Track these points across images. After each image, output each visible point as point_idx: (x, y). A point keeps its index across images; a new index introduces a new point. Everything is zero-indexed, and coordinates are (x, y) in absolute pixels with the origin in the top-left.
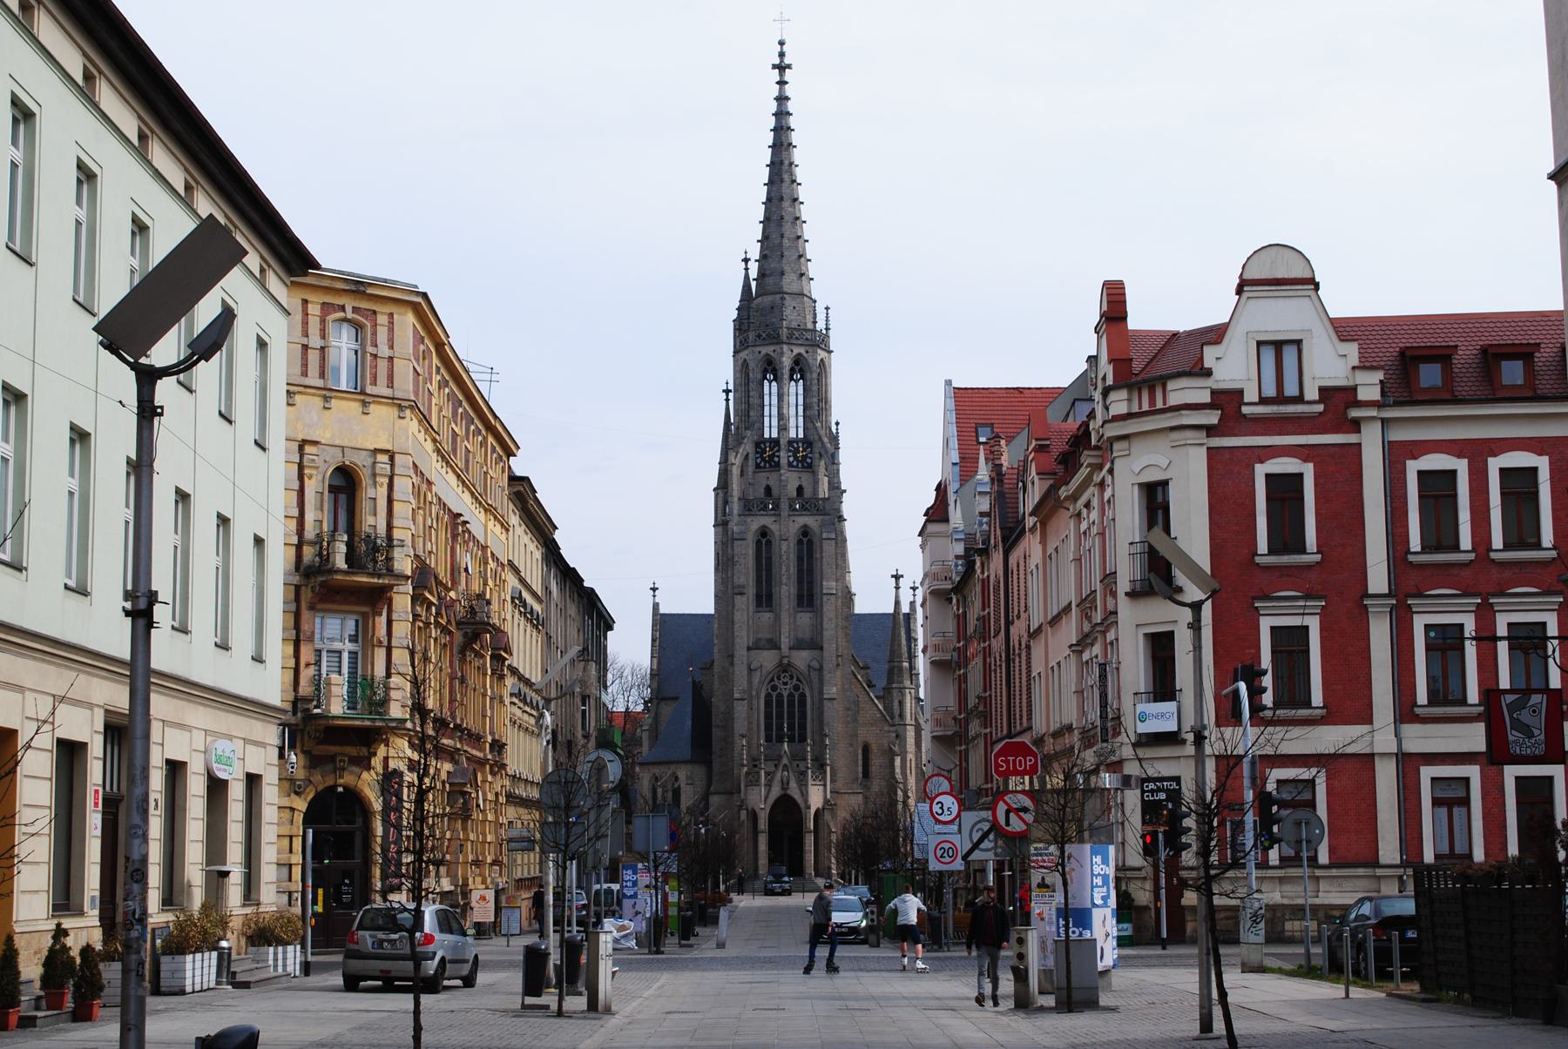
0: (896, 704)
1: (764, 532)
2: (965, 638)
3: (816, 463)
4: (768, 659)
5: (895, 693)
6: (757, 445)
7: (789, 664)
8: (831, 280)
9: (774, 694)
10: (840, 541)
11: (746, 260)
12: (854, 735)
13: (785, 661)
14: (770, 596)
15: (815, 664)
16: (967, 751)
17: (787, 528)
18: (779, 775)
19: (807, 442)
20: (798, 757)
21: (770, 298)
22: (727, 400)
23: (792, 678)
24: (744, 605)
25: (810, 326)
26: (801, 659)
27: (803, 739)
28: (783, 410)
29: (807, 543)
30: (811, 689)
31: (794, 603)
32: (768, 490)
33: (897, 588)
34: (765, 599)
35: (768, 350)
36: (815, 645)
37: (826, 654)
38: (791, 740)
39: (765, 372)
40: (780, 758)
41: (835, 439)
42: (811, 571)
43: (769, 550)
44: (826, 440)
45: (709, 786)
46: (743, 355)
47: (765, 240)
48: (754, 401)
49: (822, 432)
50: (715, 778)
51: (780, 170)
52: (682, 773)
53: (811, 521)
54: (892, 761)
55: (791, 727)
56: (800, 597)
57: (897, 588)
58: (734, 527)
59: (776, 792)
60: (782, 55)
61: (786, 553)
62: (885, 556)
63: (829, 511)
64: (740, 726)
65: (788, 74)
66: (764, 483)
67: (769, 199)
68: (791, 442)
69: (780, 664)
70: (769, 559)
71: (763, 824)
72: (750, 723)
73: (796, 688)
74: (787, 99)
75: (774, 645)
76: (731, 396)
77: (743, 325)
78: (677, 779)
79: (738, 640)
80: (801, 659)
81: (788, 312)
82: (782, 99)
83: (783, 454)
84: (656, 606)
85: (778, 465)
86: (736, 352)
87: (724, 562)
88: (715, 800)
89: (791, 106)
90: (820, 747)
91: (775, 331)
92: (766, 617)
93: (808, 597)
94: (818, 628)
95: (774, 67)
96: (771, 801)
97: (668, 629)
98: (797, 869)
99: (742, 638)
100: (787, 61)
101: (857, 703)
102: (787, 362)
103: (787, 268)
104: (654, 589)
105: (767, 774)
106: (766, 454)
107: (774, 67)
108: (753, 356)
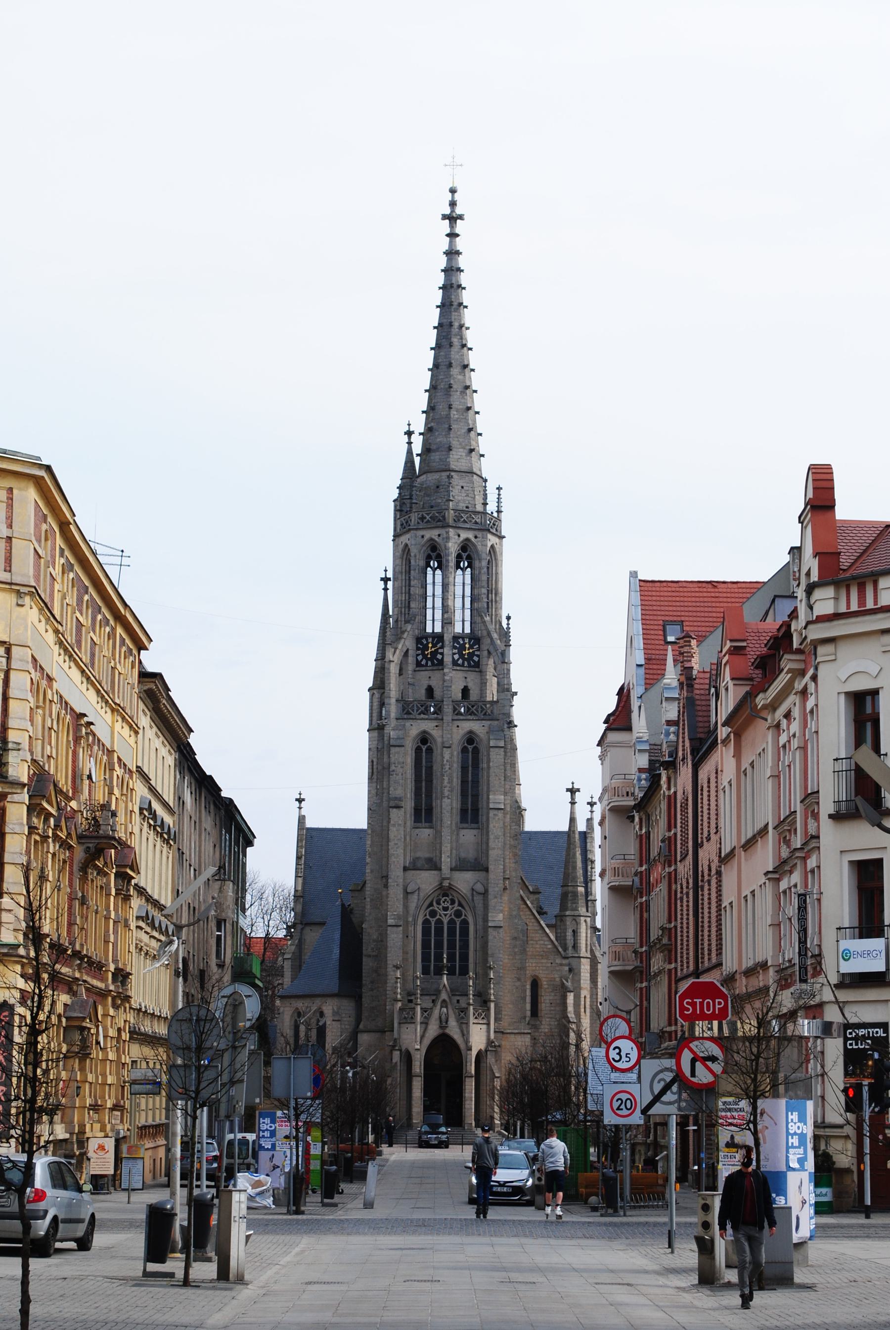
0: (569, 933)
1: (424, 738)
2: (648, 861)
3: (484, 661)
4: (426, 881)
5: (569, 921)
6: (418, 640)
7: (450, 887)
8: (506, 458)
9: (433, 921)
10: (510, 749)
11: (409, 433)
12: (522, 968)
13: (446, 883)
14: (430, 811)
15: (479, 888)
16: (648, 989)
17: (450, 734)
18: (436, 1012)
19: (475, 639)
20: (459, 992)
21: (436, 476)
22: (386, 589)
23: (453, 902)
24: (401, 820)
25: (479, 508)
26: (464, 881)
27: (464, 971)
28: (447, 603)
29: (472, 751)
30: (475, 916)
31: (457, 818)
32: (430, 691)
33: (573, 803)
34: (424, 813)
35: (433, 534)
36: (480, 866)
37: (491, 876)
38: (451, 972)
39: (429, 558)
40: (437, 993)
41: (505, 635)
42: (476, 782)
43: (430, 760)
44: (495, 636)
45: (358, 1020)
46: (404, 539)
47: (431, 410)
48: (416, 591)
49: (491, 627)
50: (365, 1014)
51: (449, 333)
52: (329, 1008)
53: (478, 727)
54: (564, 998)
55: (451, 958)
56: (463, 812)
57: (573, 803)
58: (391, 732)
59: (433, 1031)
60: (453, 204)
61: (449, 762)
62: (559, 769)
63: (498, 716)
64: (394, 956)
65: (460, 227)
66: (425, 684)
67: (436, 366)
68: (456, 638)
69: (440, 887)
70: (430, 769)
71: (418, 1066)
72: (405, 953)
73: (458, 914)
74: (458, 253)
75: (433, 865)
76: (390, 584)
77: (404, 506)
78: (322, 1014)
79: (393, 859)
80: (464, 881)
81: (455, 492)
82: (452, 253)
83: (447, 651)
84: (302, 820)
85: (441, 662)
86: (396, 536)
87: (379, 771)
88: (364, 1039)
89: (462, 262)
90: (484, 981)
91: (440, 514)
92: (425, 833)
93: (472, 812)
94: (483, 847)
95: (444, 217)
96: (427, 1042)
97: (314, 845)
98: (455, 1119)
99: (398, 857)
100: (458, 211)
101: (526, 932)
102: (453, 548)
103: (455, 443)
104: (300, 800)
105: (424, 1010)
106: (429, 650)
107: (444, 217)
108: (415, 540)
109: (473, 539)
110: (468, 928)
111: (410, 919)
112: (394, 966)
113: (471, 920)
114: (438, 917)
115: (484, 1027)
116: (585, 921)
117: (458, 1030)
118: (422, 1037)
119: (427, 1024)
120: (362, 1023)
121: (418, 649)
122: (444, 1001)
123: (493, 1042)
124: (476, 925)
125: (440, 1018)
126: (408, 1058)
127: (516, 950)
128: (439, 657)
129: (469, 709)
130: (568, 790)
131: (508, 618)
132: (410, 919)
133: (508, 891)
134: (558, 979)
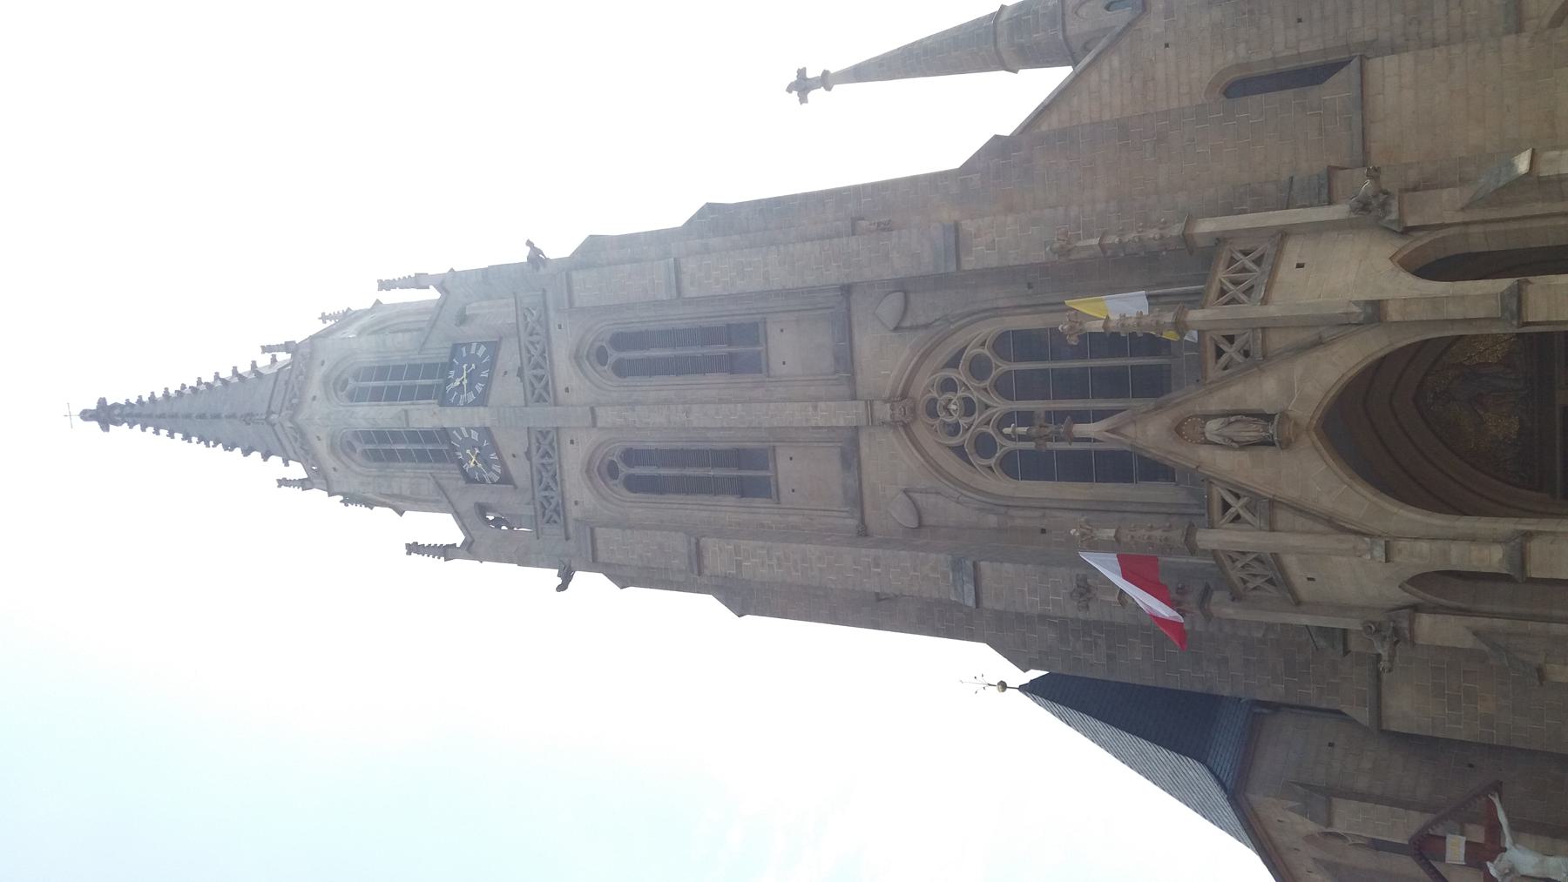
13: (884, 411)
14: (738, 457)
23: (948, 385)
26: (884, 358)
33: (826, 81)
42: (672, 337)
56: (729, 365)
69: (904, 426)
71: (1478, 544)
73: (979, 368)
85: (486, 432)
92: (788, 469)
96: (1356, 500)
109: (324, 369)
111: (992, 520)
113: (990, 329)
114: (990, 430)
115: (1294, 251)
117: (1298, 367)
118: (1334, 524)
119: (1273, 503)
121: (483, 481)
122: (1178, 430)
123: (1364, 206)
124: (997, 312)
125: (1245, 445)
126: (1442, 587)
128: (475, 436)
129: (537, 366)
130: (803, 100)
131: (385, 285)
132: (992, 520)
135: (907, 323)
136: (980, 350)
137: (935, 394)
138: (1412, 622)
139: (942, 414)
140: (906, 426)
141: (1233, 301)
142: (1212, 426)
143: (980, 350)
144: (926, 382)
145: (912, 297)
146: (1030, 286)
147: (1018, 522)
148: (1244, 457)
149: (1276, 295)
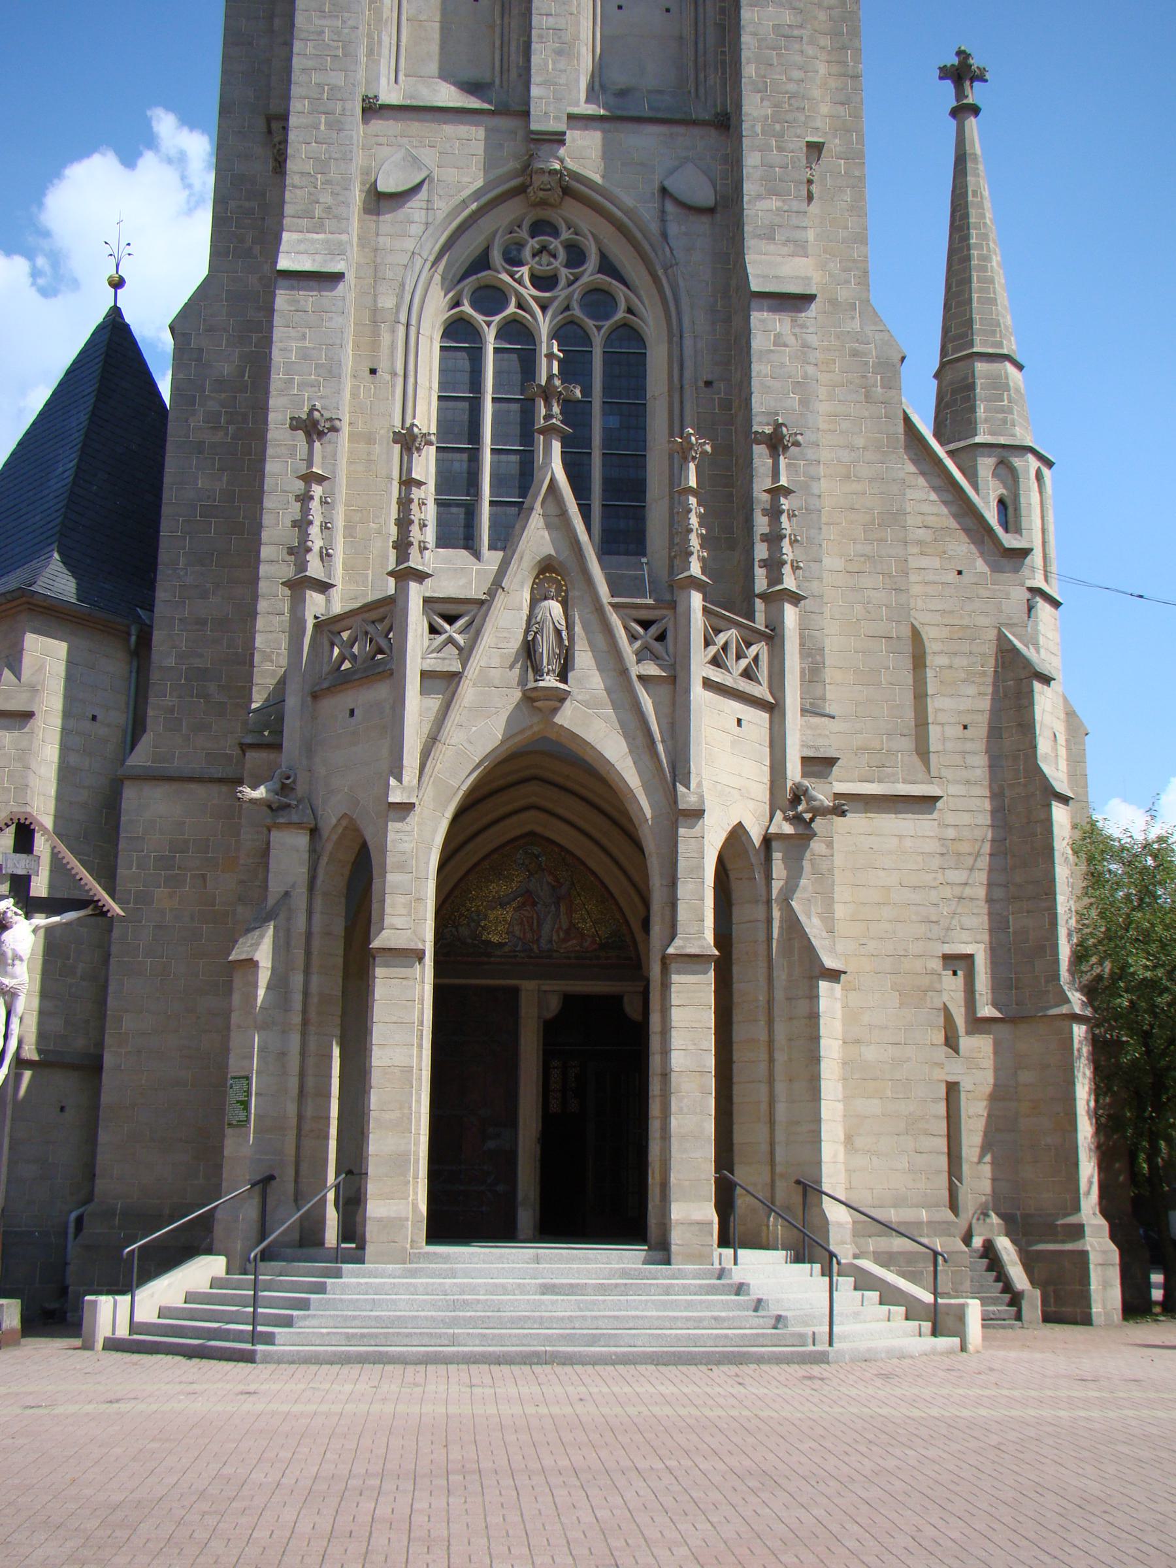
23: (576, 255)
73: (599, 301)
88: (151, 811)
110: (641, 358)
112: (296, 424)
113: (652, 325)
114: (512, 309)
115: (758, 719)
116: (1039, 476)
120: (146, 741)
124: (675, 337)
127: (860, 442)
132: (387, 302)
133: (814, 208)
134: (992, 634)
135: (670, 207)
136: (622, 306)
137: (565, 235)
138: (299, 825)
139: (533, 243)
140: (521, 190)
141: (708, 643)
142: (555, 608)
143: (622, 306)
144: (584, 227)
145: (705, 219)
146: (708, 384)
147: (386, 338)
148: (515, 643)
149: (709, 695)
